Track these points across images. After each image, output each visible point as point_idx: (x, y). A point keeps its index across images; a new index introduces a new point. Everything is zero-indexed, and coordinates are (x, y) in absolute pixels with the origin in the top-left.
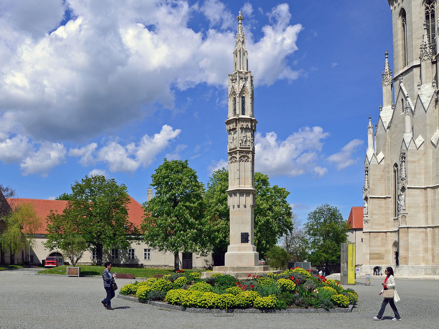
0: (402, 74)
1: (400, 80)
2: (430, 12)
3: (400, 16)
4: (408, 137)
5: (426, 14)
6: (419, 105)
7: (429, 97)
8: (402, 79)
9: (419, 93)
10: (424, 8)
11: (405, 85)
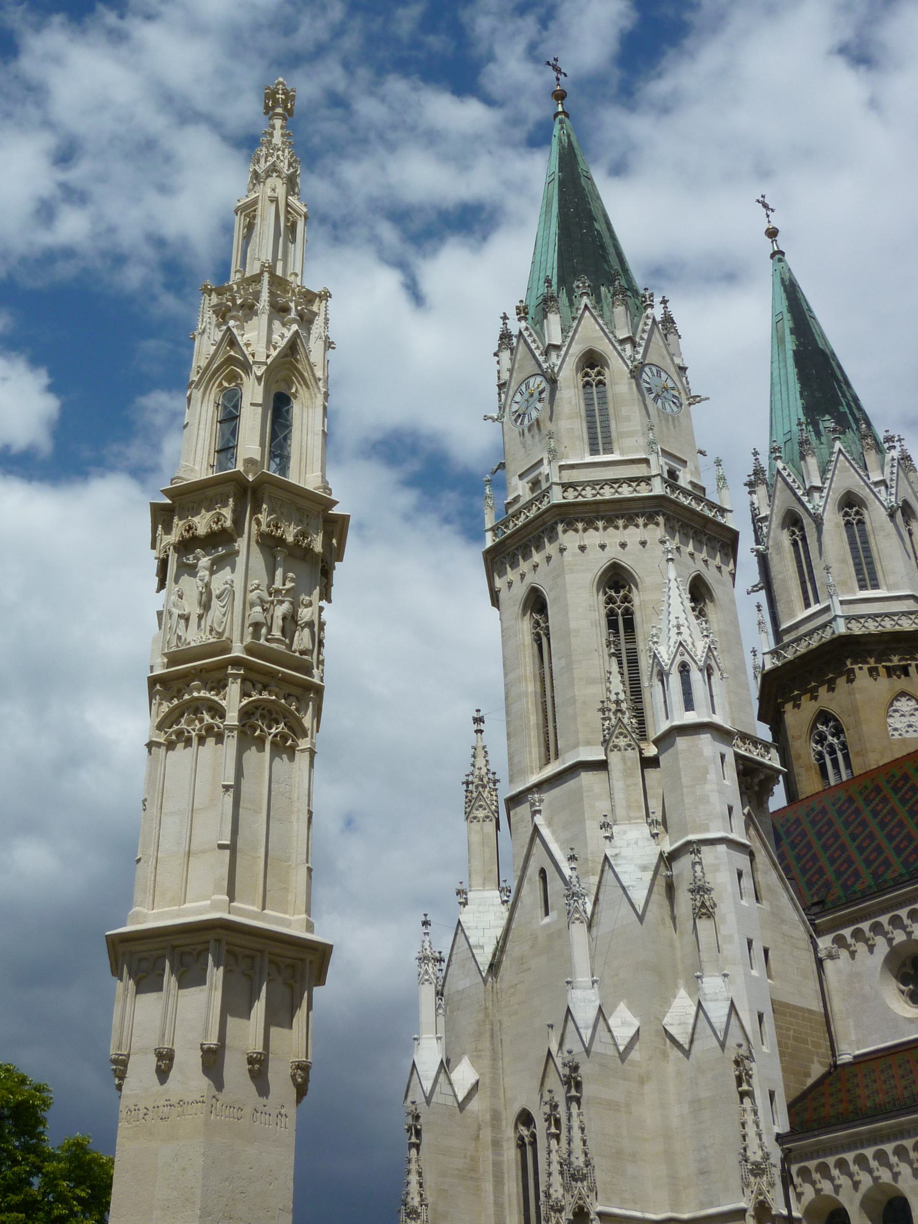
0: (539, 787)
1: (532, 805)
2: (620, 611)
3: (524, 614)
4: (584, 1002)
5: (608, 616)
6: (610, 892)
7: (644, 868)
8: (541, 801)
9: (609, 853)
10: (602, 598)
11: (549, 824)
